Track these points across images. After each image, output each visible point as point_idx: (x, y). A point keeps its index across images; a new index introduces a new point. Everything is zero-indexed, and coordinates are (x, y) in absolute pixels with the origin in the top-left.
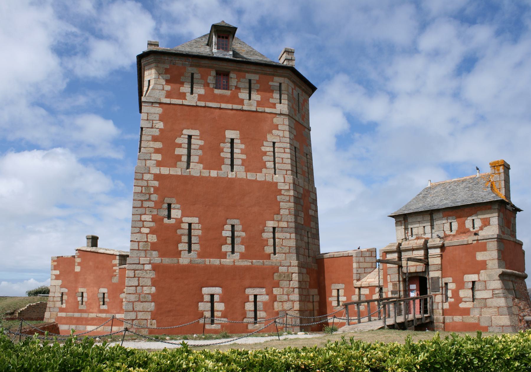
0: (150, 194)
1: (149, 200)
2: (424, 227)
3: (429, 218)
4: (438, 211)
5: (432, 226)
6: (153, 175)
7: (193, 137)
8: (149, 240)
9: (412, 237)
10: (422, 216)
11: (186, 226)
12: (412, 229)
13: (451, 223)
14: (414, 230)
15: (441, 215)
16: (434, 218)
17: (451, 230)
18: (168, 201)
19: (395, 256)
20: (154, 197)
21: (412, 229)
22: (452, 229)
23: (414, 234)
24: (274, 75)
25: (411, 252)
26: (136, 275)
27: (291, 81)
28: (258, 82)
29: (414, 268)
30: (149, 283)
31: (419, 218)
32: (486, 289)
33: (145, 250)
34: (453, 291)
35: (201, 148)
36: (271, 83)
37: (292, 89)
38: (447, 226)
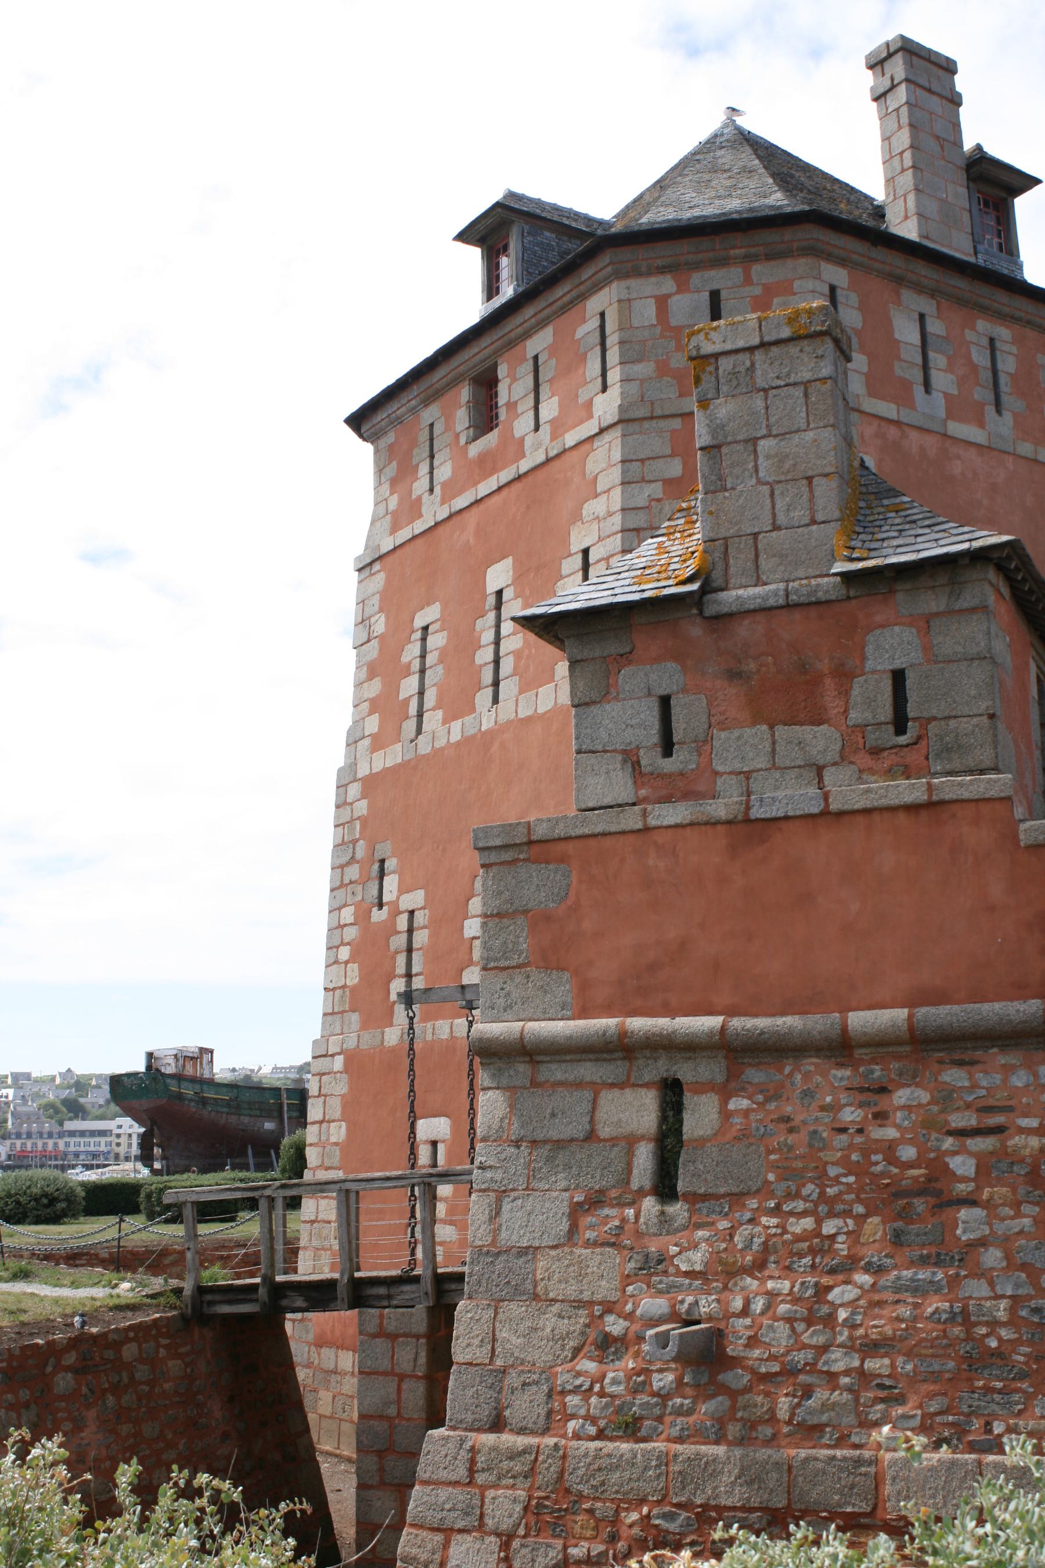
0: (354, 842)
1: (353, 860)
6: (360, 782)
7: (431, 629)
8: (348, 983)
11: (402, 923)
18: (380, 852)
20: (361, 852)
24: (583, 297)
26: (323, 1092)
27: (649, 273)
28: (552, 350)
30: (338, 1114)
33: (342, 1012)
35: (444, 653)
36: (580, 332)
37: (662, 302)
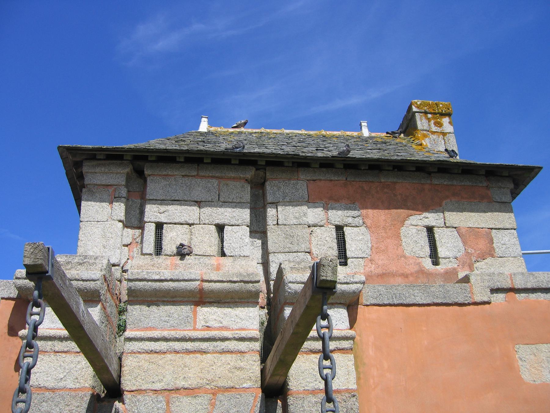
2: (220, 228)
3: (247, 197)
10: (215, 182)
12: (159, 226)
13: (339, 229)
16: (270, 198)
21: (159, 226)
22: (349, 254)
25: (185, 310)
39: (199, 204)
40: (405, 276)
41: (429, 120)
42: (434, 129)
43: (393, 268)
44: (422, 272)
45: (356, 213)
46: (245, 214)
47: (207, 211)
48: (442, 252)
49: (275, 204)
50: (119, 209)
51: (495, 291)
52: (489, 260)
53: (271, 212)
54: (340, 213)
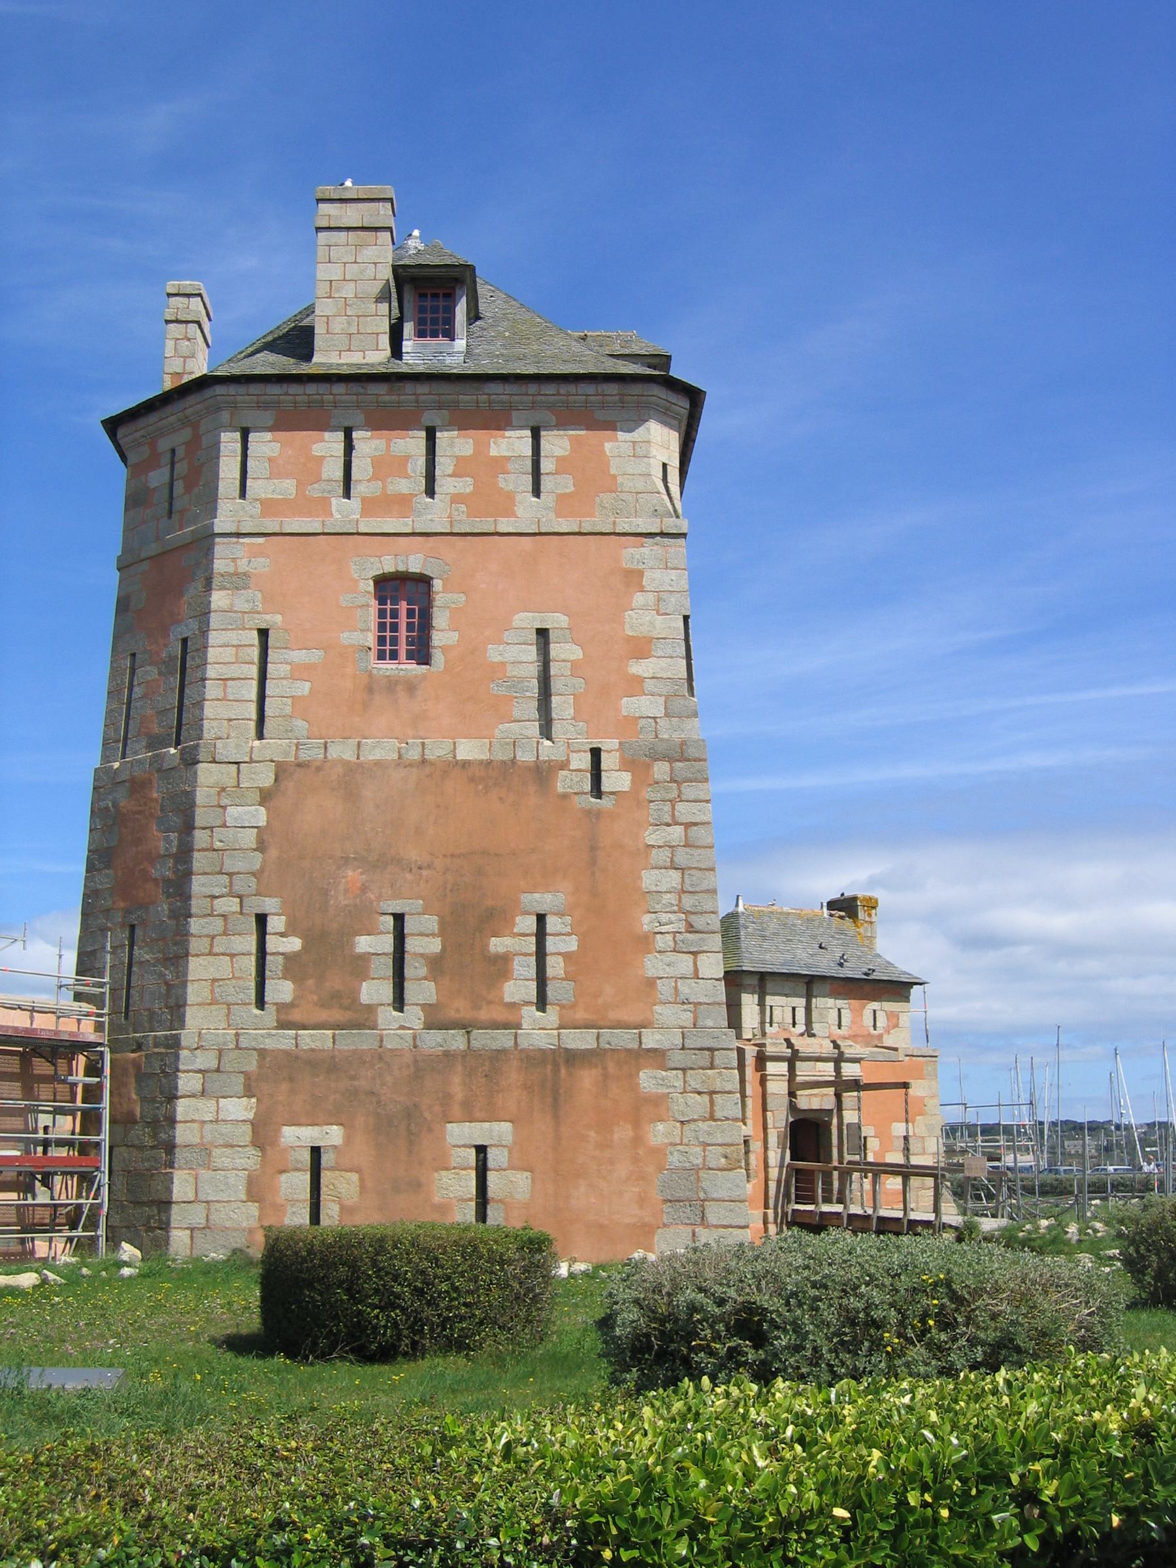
2: (794, 1009)
4: (823, 978)
5: (808, 1010)
9: (771, 1026)
12: (771, 1007)
14: (775, 1013)
15: (827, 987)
17: (840, 1026)
19: (783, 1067)
21: (771, 1007)
23: (775, 1019)
29: (809, 1101)
31: (788, 986)
32: (924, 1153)
34: (875, 1153)
38: (834, 1014)
39: (786, 995)
40: (863, 1036)
41: (865, 911)
42: (867, 919)
43: (859, 1032)
44: (869, 1035)
45: (846, 1001)
46: (802, 1001)
47: (789, 999)
48: (878, 1024)
49: (816, 997)
50: (756, 996)
51: (907, 1056)
52: (896, 1029)
53: (814, 1000)
54: (841, 1001)
